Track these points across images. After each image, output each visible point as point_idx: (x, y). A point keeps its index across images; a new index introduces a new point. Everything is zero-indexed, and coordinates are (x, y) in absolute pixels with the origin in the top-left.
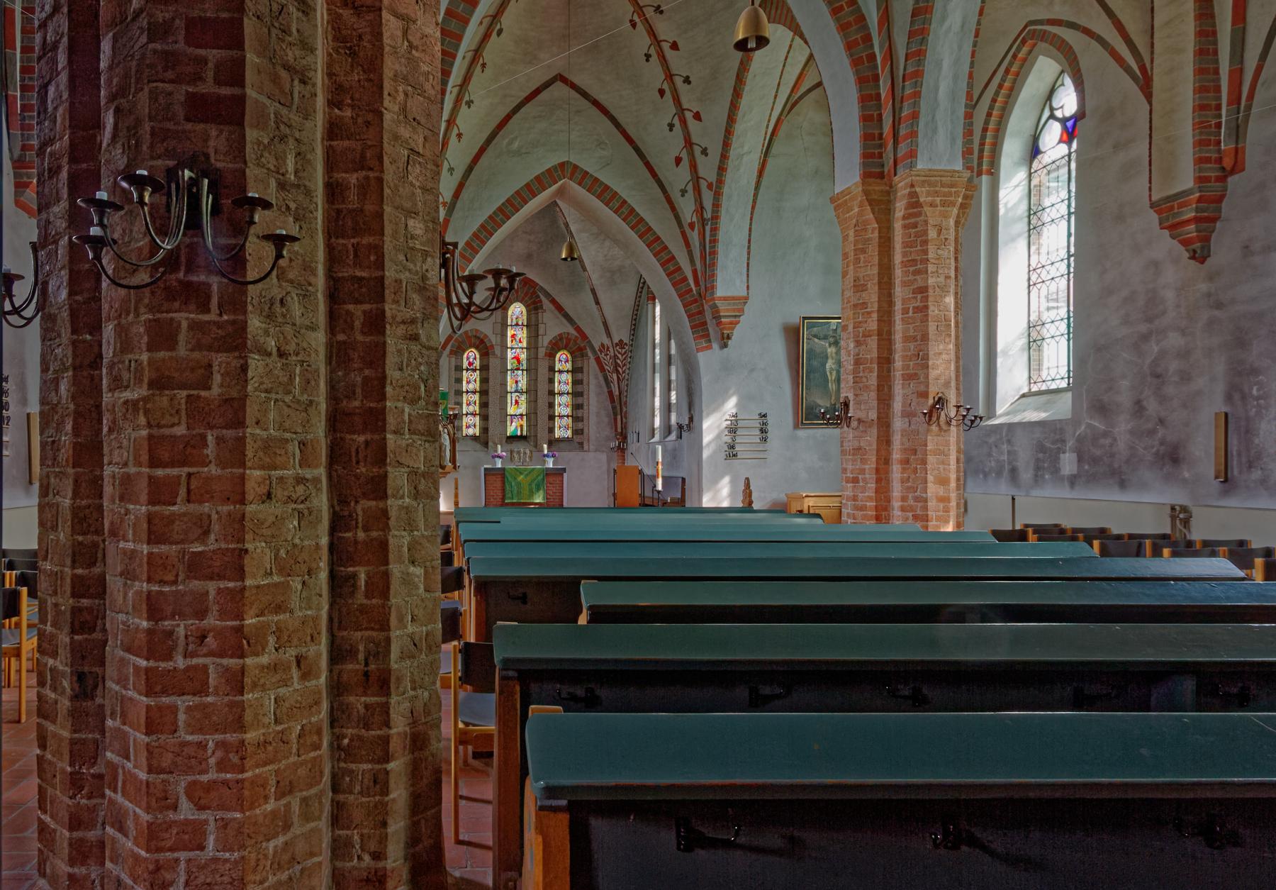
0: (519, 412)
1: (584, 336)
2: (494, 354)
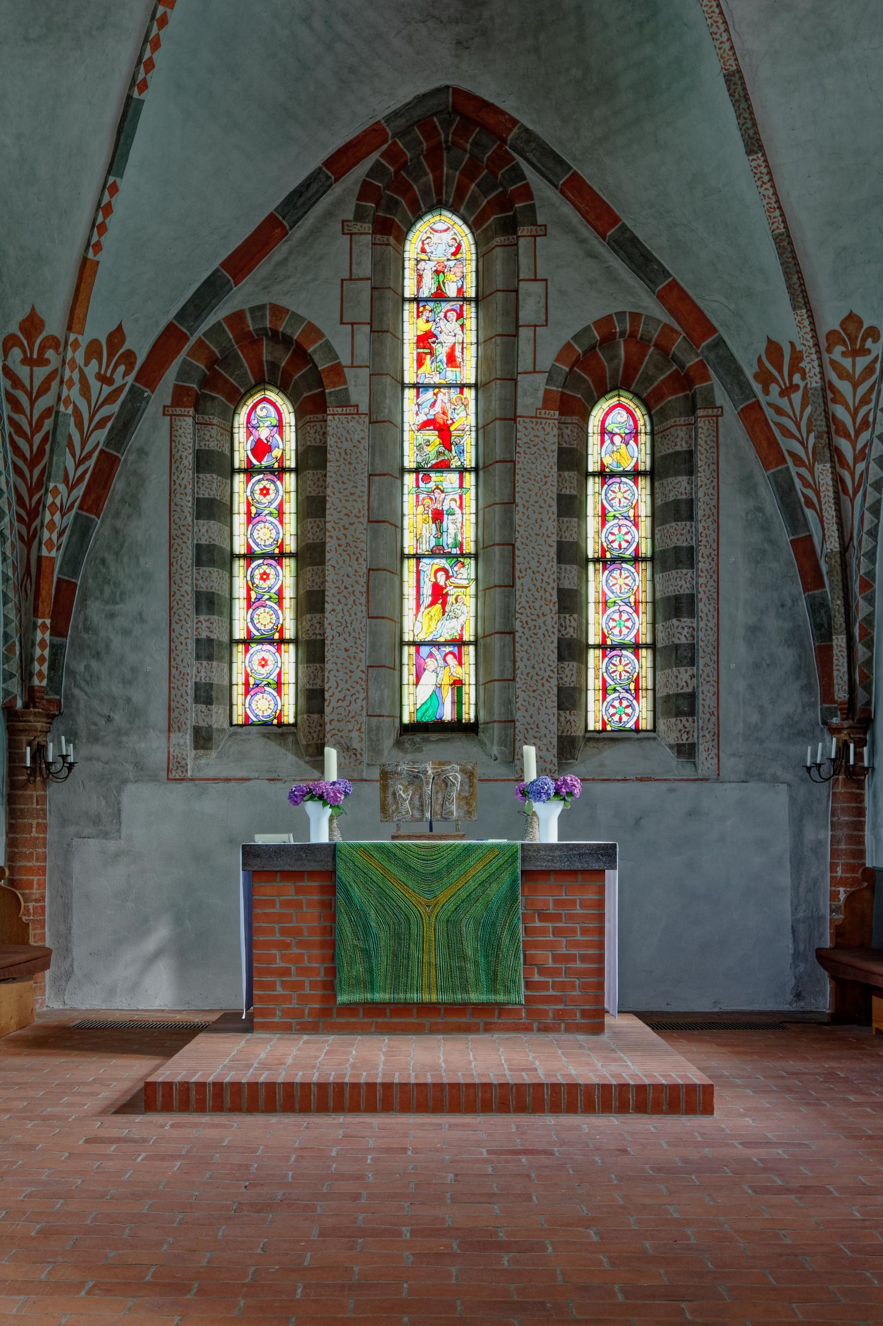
0: (447, 630)
1: (698, 325)
2: (344, 402)
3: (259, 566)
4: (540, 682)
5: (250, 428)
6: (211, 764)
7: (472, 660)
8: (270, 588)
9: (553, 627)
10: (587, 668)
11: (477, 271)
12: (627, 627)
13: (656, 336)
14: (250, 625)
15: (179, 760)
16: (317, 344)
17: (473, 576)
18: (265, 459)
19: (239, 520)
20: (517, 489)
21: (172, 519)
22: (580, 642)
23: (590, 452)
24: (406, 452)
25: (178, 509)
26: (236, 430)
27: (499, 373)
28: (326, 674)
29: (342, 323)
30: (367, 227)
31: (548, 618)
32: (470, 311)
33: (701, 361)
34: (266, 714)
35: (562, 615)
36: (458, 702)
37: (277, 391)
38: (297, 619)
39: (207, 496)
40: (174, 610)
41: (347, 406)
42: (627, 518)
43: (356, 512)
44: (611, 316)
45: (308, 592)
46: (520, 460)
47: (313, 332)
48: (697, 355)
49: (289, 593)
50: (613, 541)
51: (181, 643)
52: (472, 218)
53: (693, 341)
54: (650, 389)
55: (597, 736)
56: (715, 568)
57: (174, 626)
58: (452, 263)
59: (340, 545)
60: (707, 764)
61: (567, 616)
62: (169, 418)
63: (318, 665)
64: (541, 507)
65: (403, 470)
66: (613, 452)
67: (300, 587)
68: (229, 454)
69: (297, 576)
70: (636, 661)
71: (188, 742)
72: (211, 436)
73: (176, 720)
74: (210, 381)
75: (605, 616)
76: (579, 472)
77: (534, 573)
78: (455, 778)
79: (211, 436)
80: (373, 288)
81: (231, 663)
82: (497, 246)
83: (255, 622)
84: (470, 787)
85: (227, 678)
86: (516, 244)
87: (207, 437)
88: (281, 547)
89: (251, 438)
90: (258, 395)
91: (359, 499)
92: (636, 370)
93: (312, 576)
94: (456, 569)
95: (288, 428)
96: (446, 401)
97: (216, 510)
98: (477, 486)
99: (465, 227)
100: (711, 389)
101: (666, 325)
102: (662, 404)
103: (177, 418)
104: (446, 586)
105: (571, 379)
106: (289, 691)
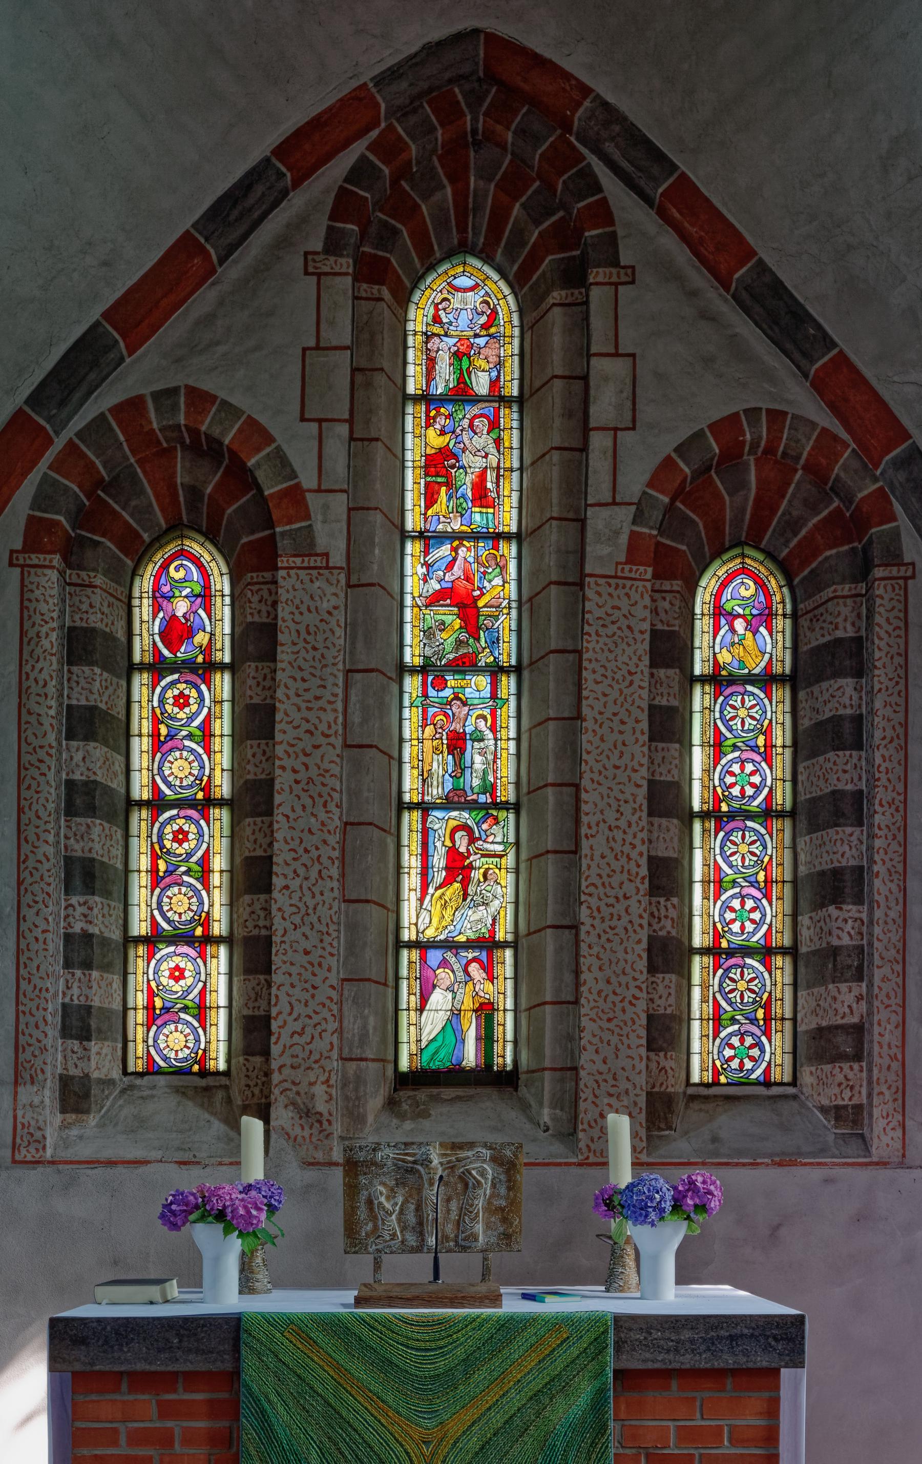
0: (470, 923)
2: (306, 546)
3: (172, 818)
4: (619, 1006)
5: (160, 599)
6: (89, 1136)
7: (509, 972)
8: (189, 855)
9: (641, 917)
10: (690, 986)
11: (522, 355)
12: (753, 921)
13: (808, 449)
14: (156, 913)
15: (31, 1130)
16: (264, 453)
17: (512, 839)
18: (182, 650)
19: (141, 746)
20: (585, 693)
21: (23, 736)
22: (680, 942)
23: (697, 643)
24: (408, 640)
25: (33, 719)
26: (136, 602)
27: (555, 509)
28: (274, 990)
29: (303, 419)
30: (346, 264)
31: (633, 902)
32: (509, 418)
33: (881, 489)
34: (181, 1055)
35: (654, 899)
36: (487, 1039)
37: (202, 539)
38: (232, 904)
39: (83, 702)
40: (25, 884)
41: (310, 555)
42: (754, 748)
43: (323, 727)
44: (736, 414)
45: (247, 858)
46: (590, 646)
47: (257, 434)
48: (875, 479)
49: (218, 863)
50: (733, 785)
51: (37, 939)
52: (515, 268)
53: (869, 457)
54: (795, 541)
55: (704, 1091)
56: (900, 823)
57: (25, 911)
58: (481, 341)
59: (297, 782)
60: (886, 1140)
61: (662, 900)
62: (19, 570)
63: (262, 977)
64: (623, 722)
65: (402, 669)
66: (733, 644)
67: (237, 852)
68: (123, 639)
69: (232, 837)
70: (766, 975)
71: (47, 1101)
72: (91, 606)
73: (27, 1065)
74: (92, 516)
75: (719, 903)
76: (682, 670)
77: (610, 829)
78: (483, 1173)
79: (91, 606)
80: (355, 370)
81: (125, 974)
82: (554, 305)
83: (165, 908)
84: (509, 1189)
85: (118, 999)
86: (586, 303)
87: (84, 607)
88: (207, 789)
89: (161, 615)
90: (172, 546)
91: (329, 707)
92: (774, 510)
93: (253, 833)
94: (485, 826)
95: (219, 599)
96: (471, 560)
97: (101, 726)
98: (519, 695)
99: (502, 284)
100: (896, 535)
101: (824, 430)
102: (814, 565)
103: (32, 570)
104: (469, 854)
105: (671, 520)
106: (220, 1020)
